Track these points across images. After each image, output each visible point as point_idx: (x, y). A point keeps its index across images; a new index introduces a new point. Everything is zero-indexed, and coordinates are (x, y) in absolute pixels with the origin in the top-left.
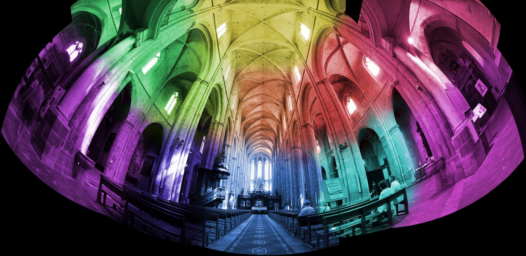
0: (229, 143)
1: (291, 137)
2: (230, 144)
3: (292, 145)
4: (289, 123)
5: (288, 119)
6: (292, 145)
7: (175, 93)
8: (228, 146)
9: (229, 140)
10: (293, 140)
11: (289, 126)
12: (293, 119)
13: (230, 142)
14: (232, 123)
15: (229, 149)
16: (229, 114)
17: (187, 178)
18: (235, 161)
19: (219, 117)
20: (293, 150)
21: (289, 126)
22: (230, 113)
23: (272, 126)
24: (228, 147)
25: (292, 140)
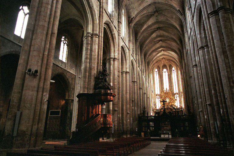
0: (114, 56)
1: (197, 32)
2: (116, 57)
3: (199, 43)
4: (193, 12)
5: (192, 6)
6: (199, 43)
7: (22, 9)
8: (114, 59)
9: (114, 51)
10: (200, 37)
11: (193, 17)
12: (197, 4)
13: (116, 54)
14: (113, 30)
15: (116, 63)
16: (105, 18)
17: (72, 108)
18: (128, 75)
19: (92, 26)
20: (201, 52)
21: (193, 17)
22: (105, 18)
23: (172, 21)
24: (114, 61)
25: (199, 36)
